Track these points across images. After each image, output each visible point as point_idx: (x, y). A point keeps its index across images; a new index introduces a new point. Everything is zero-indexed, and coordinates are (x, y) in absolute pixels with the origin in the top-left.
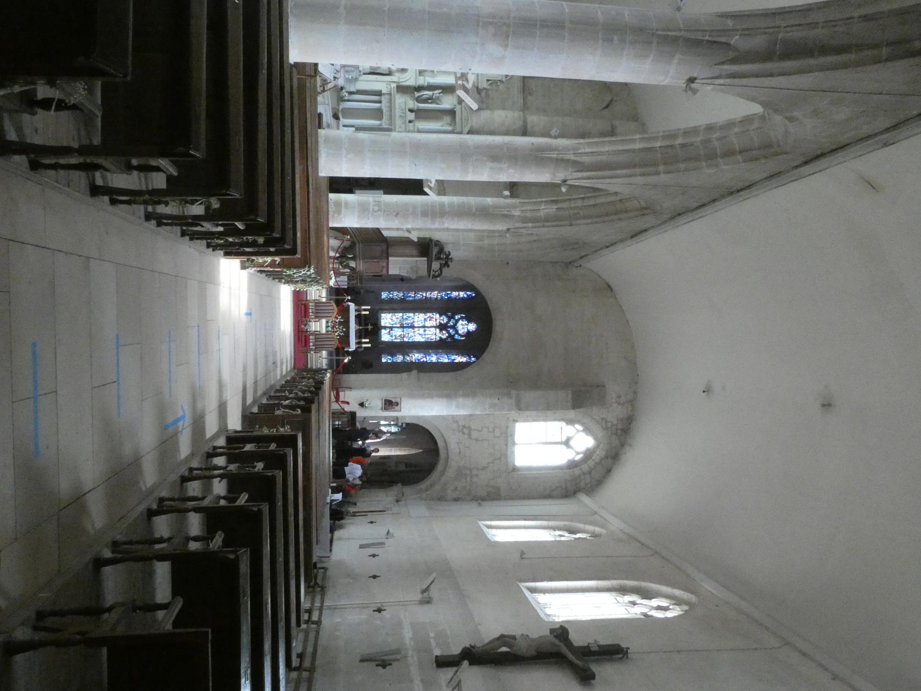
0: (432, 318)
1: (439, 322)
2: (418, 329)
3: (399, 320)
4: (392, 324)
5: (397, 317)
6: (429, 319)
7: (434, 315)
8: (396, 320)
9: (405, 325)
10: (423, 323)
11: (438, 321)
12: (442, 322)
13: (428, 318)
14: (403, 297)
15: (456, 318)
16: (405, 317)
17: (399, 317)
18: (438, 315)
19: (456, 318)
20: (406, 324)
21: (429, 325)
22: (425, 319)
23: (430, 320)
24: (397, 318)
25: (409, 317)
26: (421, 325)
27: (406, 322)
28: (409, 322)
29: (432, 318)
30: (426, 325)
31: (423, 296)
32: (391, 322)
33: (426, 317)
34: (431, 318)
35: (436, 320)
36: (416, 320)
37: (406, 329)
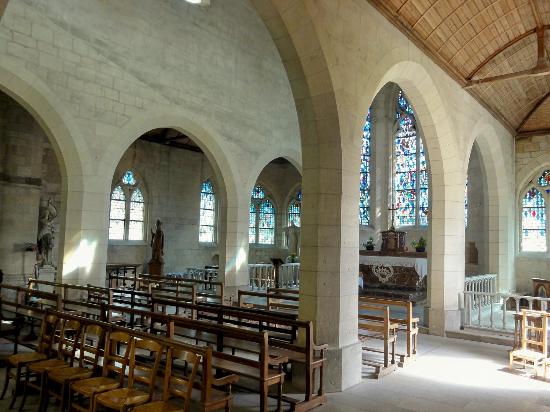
0: (403, 143)
1: (410, 130)
2: (421, 165)
3: (407, 197)
4: (413, 207)
5: (401, 201)
6: (405, 148)
7: (399, 141)
8: (407, 202)
9: (415, 187)
10: (412, 156)
11: (408, 133)
12: (410, 126)
13: (403, 150)
14: (366, 192)
15: (405, 104)
16: (401, 188)
17: (401, 197)
18: (401, 135)
19: (405, 104)
20: (412, 186)
21: (414, 146)
22: (405, 155)
23: (408, 147)
24: (404, 200)
25: (402, 180)
26: (414, 160)
27: (409, 184)
28: (409, 180)
29: (403, 143)
30: (415, 151)
31: (364, 159)
32: (408, 211)
33: (402, 153)
34: (405, 145)
35: (407, 136)
36: (407, 169)
37: (421, 183)
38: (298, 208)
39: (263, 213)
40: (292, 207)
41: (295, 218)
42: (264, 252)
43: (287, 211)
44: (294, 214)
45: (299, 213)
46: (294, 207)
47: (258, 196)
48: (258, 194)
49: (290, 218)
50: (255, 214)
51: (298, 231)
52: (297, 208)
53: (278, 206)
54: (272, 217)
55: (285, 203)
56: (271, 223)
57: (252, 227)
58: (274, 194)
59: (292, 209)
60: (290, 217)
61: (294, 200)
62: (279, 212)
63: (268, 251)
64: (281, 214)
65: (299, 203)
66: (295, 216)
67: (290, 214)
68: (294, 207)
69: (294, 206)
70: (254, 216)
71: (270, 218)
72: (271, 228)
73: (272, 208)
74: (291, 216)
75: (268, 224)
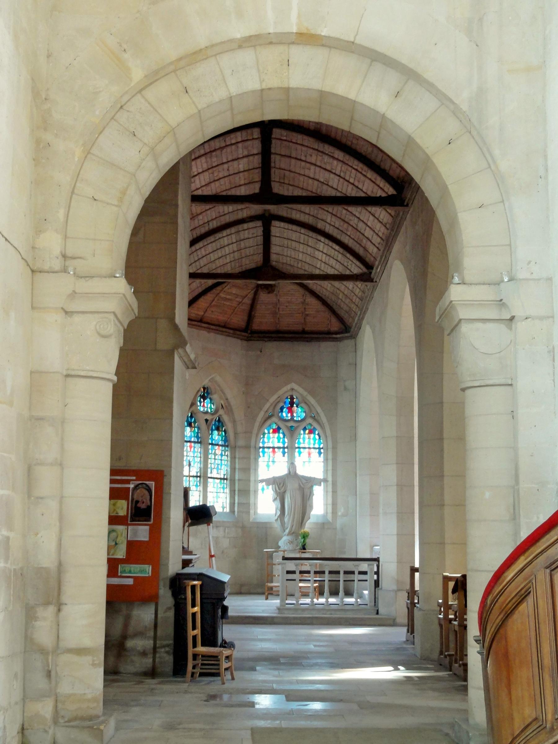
38: (281, 435)
39: (212, 444)
40: (264, 434)
41: (274, 458)
42: (221, 529)
43: (257, 441)
44: (269, 448)
45: (284, 448)
46: (269, 433)
47: (204, 406)
48: (204, 401)
49: (260, 457)
50: (199, 445)
51: (309, 485)
52: (279, 436)
53: (240, 429)
54: (223, 454)
55: (257, 424)
56: (223, 466)
57: (195, 475)
58: (233, 402)
59: (264, 437)
60: (261, 454)
61: (274, 419)
62: (241, 443)
63: (228, 527)
64: (247, 447)
65: (287, 427)
66: (274, 452)
67: (260, 448)
68: (269, 433)
69: (271, 431)
70: (198, 450)
71: (222, 455)
72: (222, 477)
73: (223, 433)
74: (264, 453)
75: (218, 469)
